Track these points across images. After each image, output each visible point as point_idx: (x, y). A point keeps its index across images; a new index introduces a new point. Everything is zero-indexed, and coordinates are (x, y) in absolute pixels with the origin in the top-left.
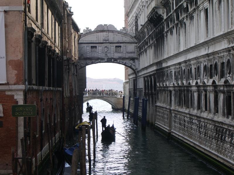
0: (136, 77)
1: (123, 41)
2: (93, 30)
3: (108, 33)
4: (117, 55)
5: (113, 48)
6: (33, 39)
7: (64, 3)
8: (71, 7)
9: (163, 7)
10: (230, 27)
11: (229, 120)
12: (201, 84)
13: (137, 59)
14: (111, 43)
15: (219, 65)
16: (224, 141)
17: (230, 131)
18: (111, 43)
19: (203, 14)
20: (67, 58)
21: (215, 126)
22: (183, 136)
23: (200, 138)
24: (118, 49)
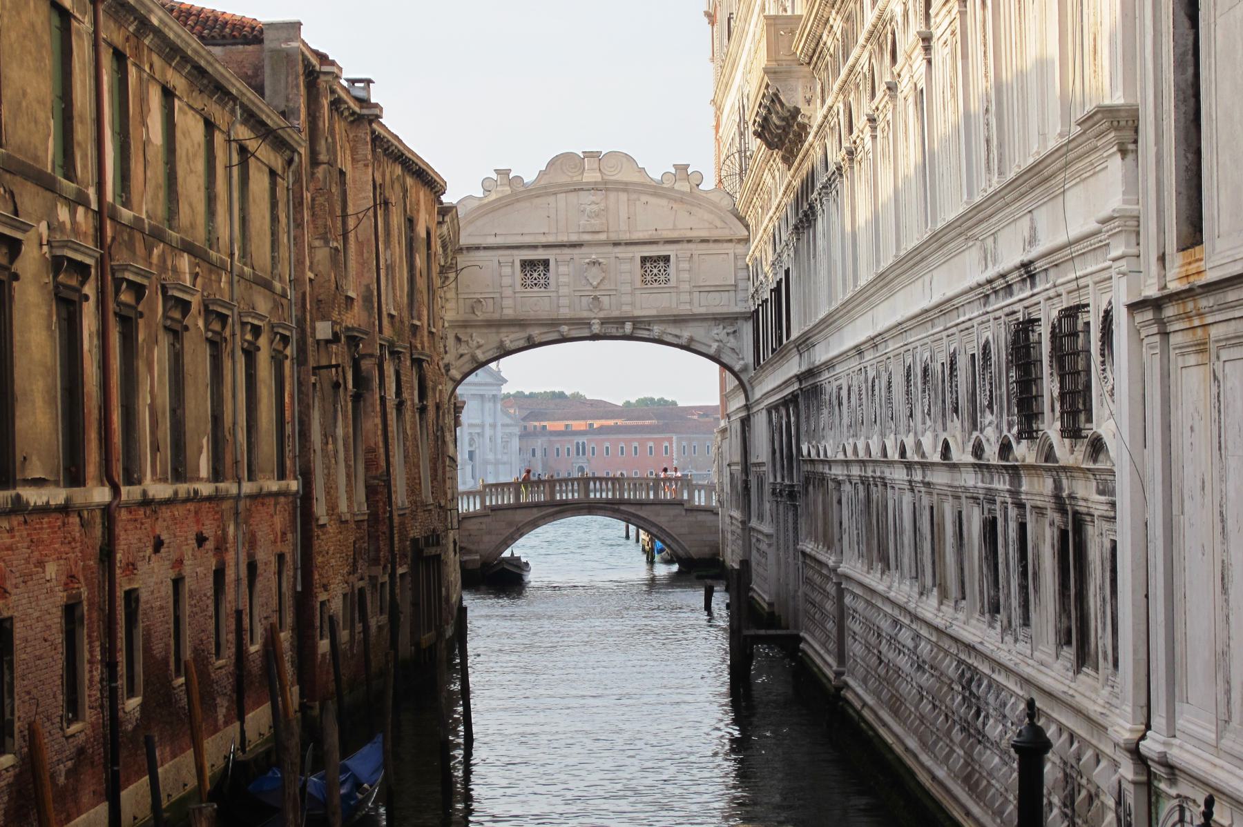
0: (747, 407)
2: (529, 177)
4: (648, 304)
5: (628, 264)
7: (307, 64)
8: (368, 82)
11: (992, 632)
12: (916, 459)
14: (616, 244)
16: (980, 737)
17: (1000, 688)
18: (616, 244)
20: (335, 334)
21: (961, 662)
22: (876, 708)
24: (655, 271)
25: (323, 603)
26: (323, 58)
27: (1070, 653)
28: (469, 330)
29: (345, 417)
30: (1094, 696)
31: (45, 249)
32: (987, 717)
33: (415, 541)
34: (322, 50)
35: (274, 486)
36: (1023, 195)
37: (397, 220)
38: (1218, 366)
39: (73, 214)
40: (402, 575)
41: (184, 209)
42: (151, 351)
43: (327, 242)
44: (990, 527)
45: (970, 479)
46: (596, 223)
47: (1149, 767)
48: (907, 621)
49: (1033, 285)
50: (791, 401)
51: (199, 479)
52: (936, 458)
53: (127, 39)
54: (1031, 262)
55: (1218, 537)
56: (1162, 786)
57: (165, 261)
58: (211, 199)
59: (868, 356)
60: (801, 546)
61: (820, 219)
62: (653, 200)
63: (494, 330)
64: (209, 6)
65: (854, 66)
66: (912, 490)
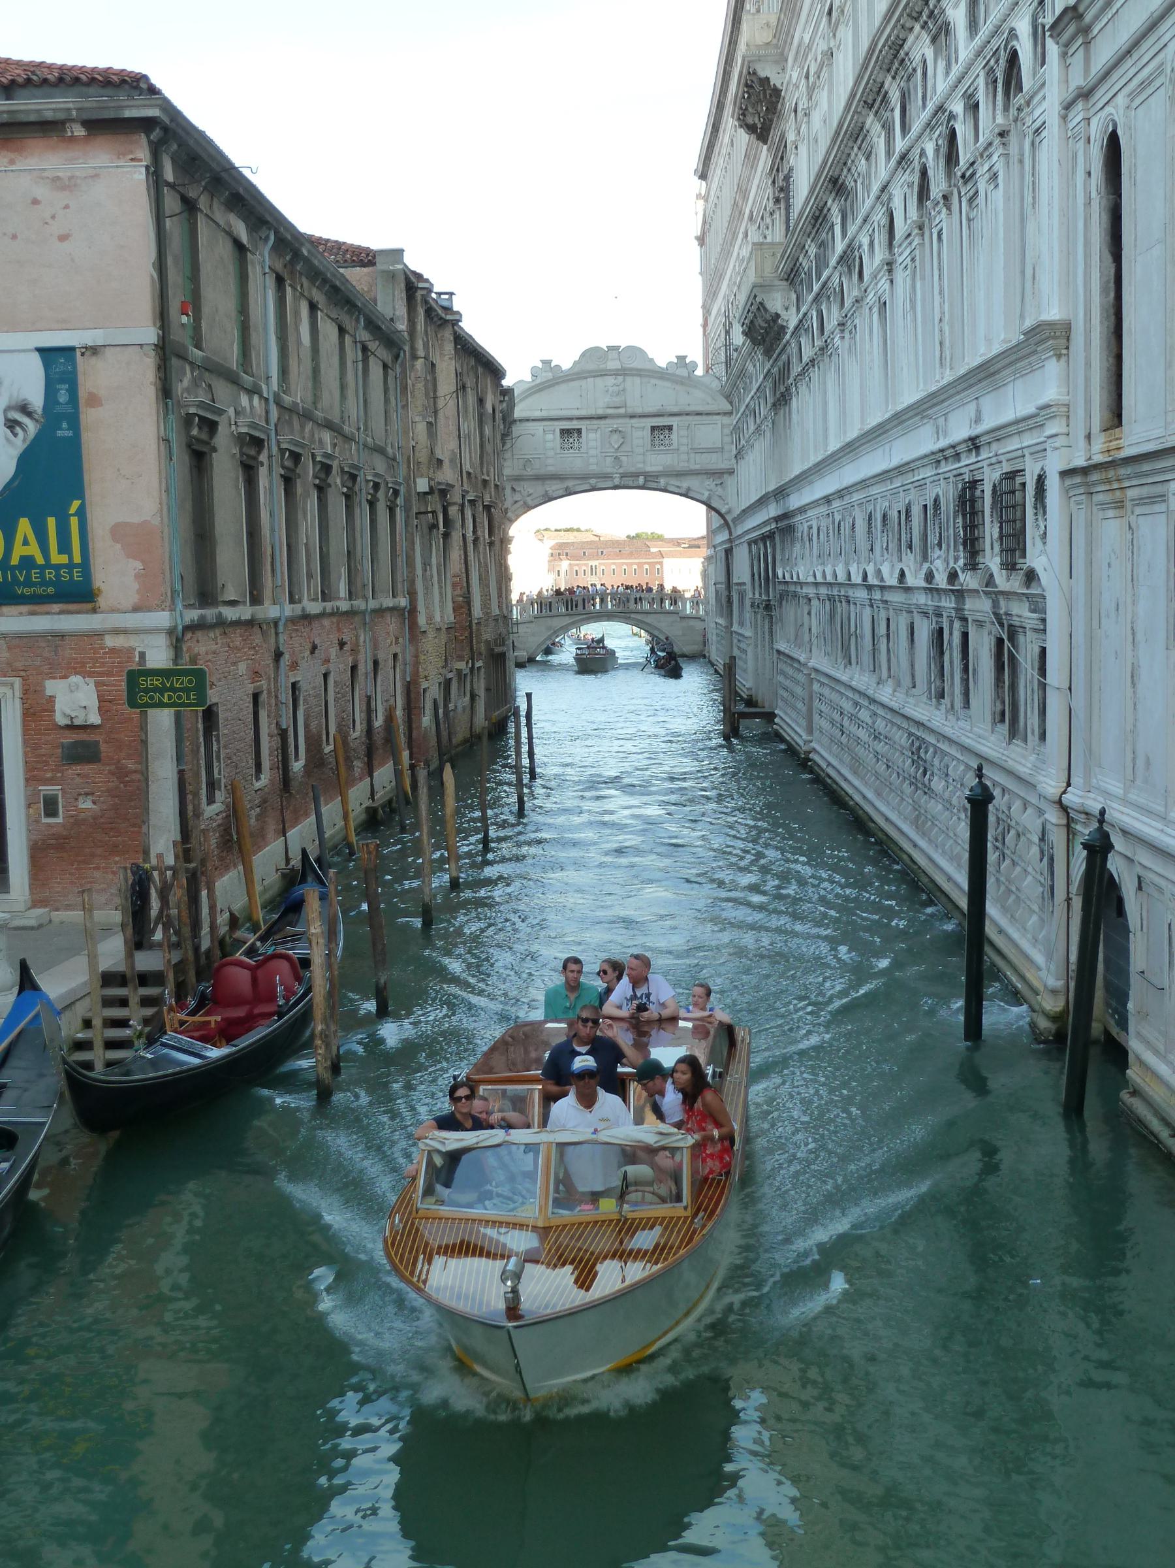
0: (730, 541)
1: (675, 409)
3: (620, 378)
4: (656, 462)
5: (640, 433)
6: (223, 439)
8: (451, 294)
9: (784, 283)
10: (937, 378)
11: (938, 713)
12: (876, 582)
13: (731, 472)
14: (632, 417)
15: (916, 511)
16: (928, 791)
17: (944, 754)
19: (875, 316)
20: (431, 488)
21: (911, 734)
22: (838, 767)
23: (877, 775)
25: (425, 690)
26: (419, 276)
27: (1004, 729)
28: (522, 483)
29: (438, 550)
30: (1023, 761)
31: (233, 427)
32: (932, 775)
33: (487, 642)
34: (418, 271)
35: (389, 602)
36: (971, 386)
37: (471, 399)
38: (1133, 519)
39: (251, 401)
40: (479, 668)
41: (325, 395)
42: (305, 503)
43: (424, 418)
44: (939, 636)
45: (922, 599)
46: (617, 400)
47: (1068, 814)
48: (866, 703)
49: (978, 454)
50: (768, 537)
51: (339, 598)
52: (893, 581)
53: (285, 266)
54: (977, 437)
55: (1130, 647)
56: (1079, 827)
57: (313, 435)
58: (343, 387)
59: (836, 504)
60: (776, 646)
61: (794, 399)
62: (659, 383)
63: (540, 482)
64: (333, 237)
65: (825, 283)
66: (872, 606)
